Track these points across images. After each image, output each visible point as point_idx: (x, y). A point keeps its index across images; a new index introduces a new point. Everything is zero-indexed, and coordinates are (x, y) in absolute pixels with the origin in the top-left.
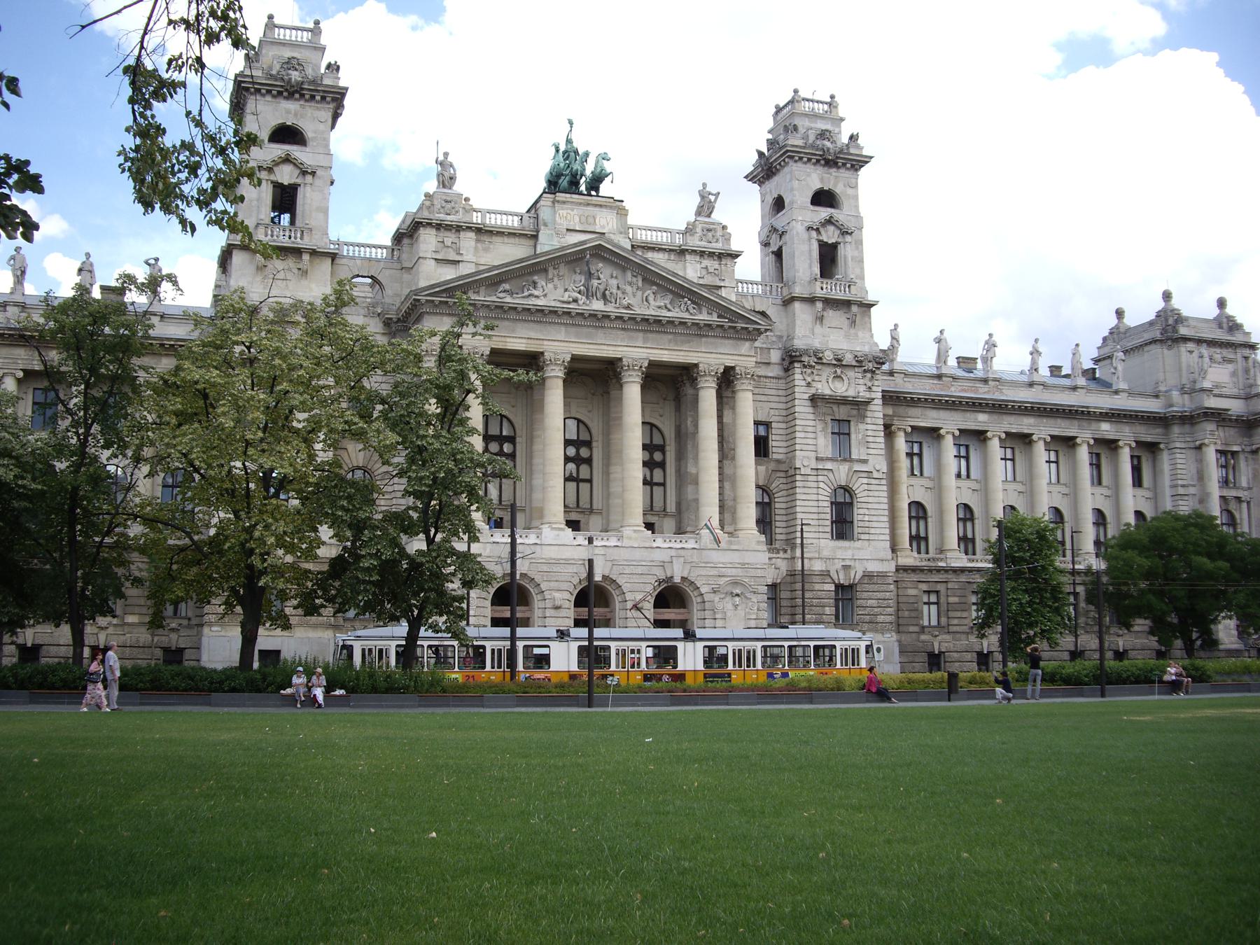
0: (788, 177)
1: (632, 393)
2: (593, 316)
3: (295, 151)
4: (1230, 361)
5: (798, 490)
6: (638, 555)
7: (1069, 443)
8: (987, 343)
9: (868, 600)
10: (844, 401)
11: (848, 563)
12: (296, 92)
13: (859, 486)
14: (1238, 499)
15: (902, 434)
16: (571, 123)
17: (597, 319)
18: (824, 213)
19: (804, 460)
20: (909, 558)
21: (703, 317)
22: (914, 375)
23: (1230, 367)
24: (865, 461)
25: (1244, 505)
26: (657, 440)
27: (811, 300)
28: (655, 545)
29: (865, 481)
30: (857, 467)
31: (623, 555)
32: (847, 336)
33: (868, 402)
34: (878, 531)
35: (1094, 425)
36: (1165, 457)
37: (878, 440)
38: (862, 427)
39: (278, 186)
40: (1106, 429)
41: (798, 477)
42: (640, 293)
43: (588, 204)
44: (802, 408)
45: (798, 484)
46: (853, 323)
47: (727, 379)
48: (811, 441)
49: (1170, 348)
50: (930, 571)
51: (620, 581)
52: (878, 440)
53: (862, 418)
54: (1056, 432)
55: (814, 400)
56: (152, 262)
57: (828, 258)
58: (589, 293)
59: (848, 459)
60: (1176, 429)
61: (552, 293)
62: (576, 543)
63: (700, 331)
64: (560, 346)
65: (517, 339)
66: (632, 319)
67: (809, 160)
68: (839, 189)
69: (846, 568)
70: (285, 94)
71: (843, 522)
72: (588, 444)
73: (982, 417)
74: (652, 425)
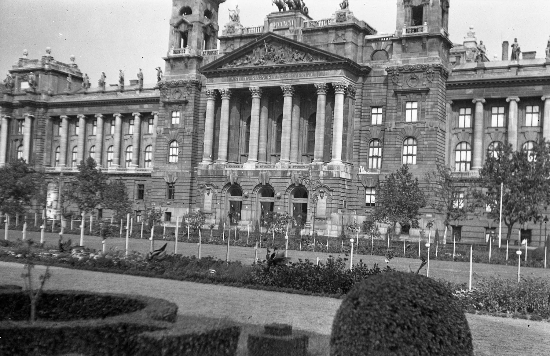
2: (266, 69)
21: (319, 61)
47: (331, 91)
50: (461, 181)
58: (268, 58)
64: (255, 84)
65: (239, 84)
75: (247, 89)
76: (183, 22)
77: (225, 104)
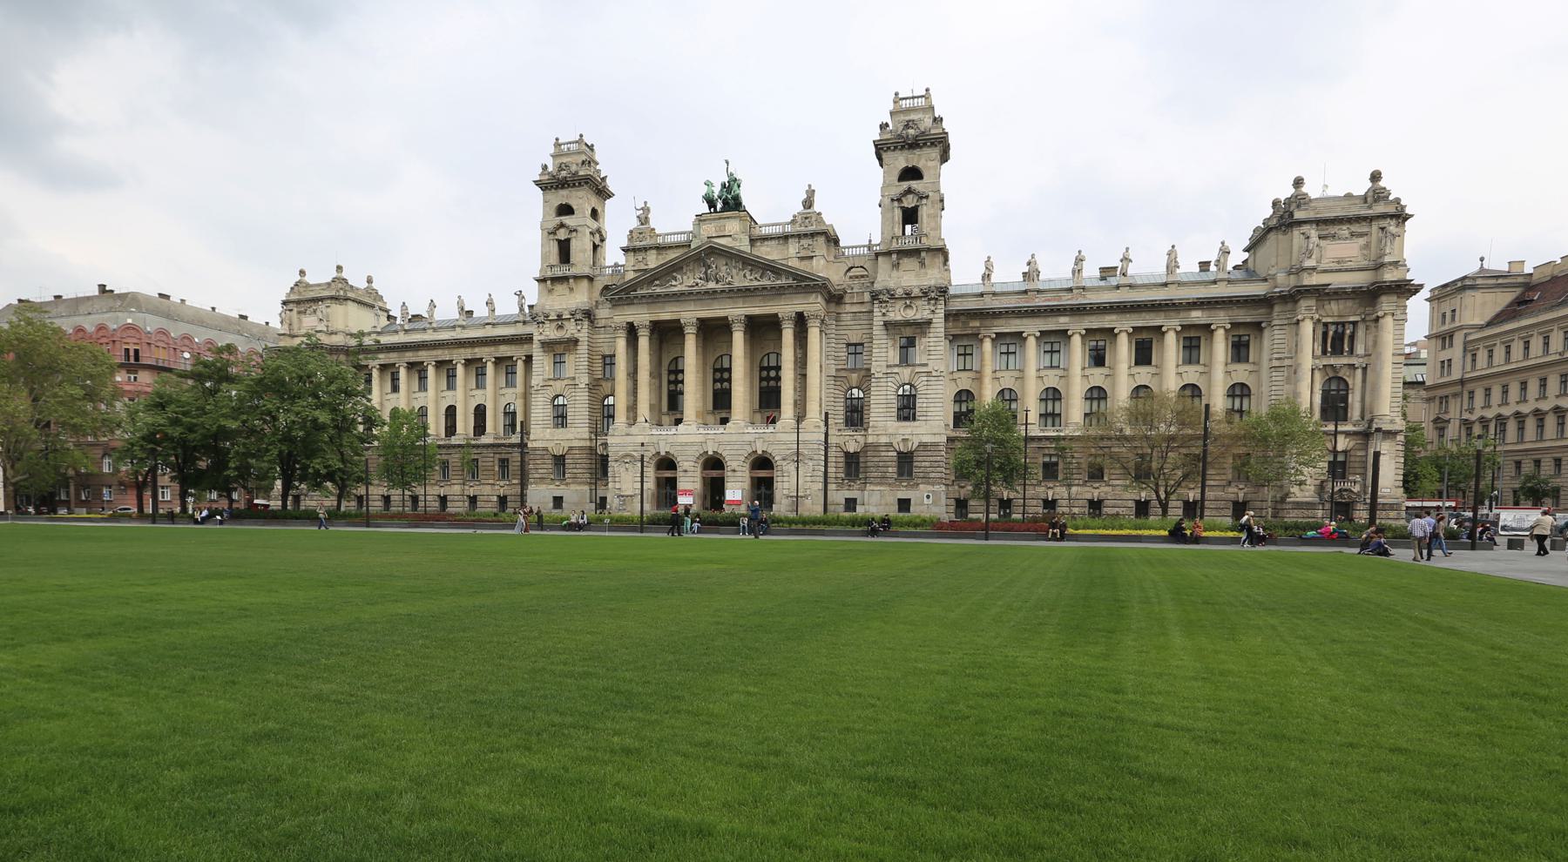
1: (738, 338)
4: (1361, 235)
6: (734, 438)
7: (1064, 334)
9: (921, 463)
10: (907, 324)
13: (921, 382)
14: (1352, 367)
17: (712, 295)
19: (877, 368)
21: (783, 281)
22: (1003, 294)
23: (1362, 241)
24: (925, 365)
25: (1359, 372)
31: (726, 438)
33: (929, 322)
35: (1182, 314)
36: (1266, 333)
39: (559, 241)
40: (1197, 316)
44: (878, 331)
46: (922, 264)
47: (801, 321)
48: (884, 353)
49: (1285, 232)
53: (924, 334)
54: (1140, 324)
55: (887, 325)
60: (1277, 308)
61: (684, 282)
63: (779, 292)
64: (689, 315)
65: (666, 314)
66: (731, 291)
71: (907, 409)
73: (1063, 320)
75: (678, 321)
76: (562, 225)
77: (644, 342)
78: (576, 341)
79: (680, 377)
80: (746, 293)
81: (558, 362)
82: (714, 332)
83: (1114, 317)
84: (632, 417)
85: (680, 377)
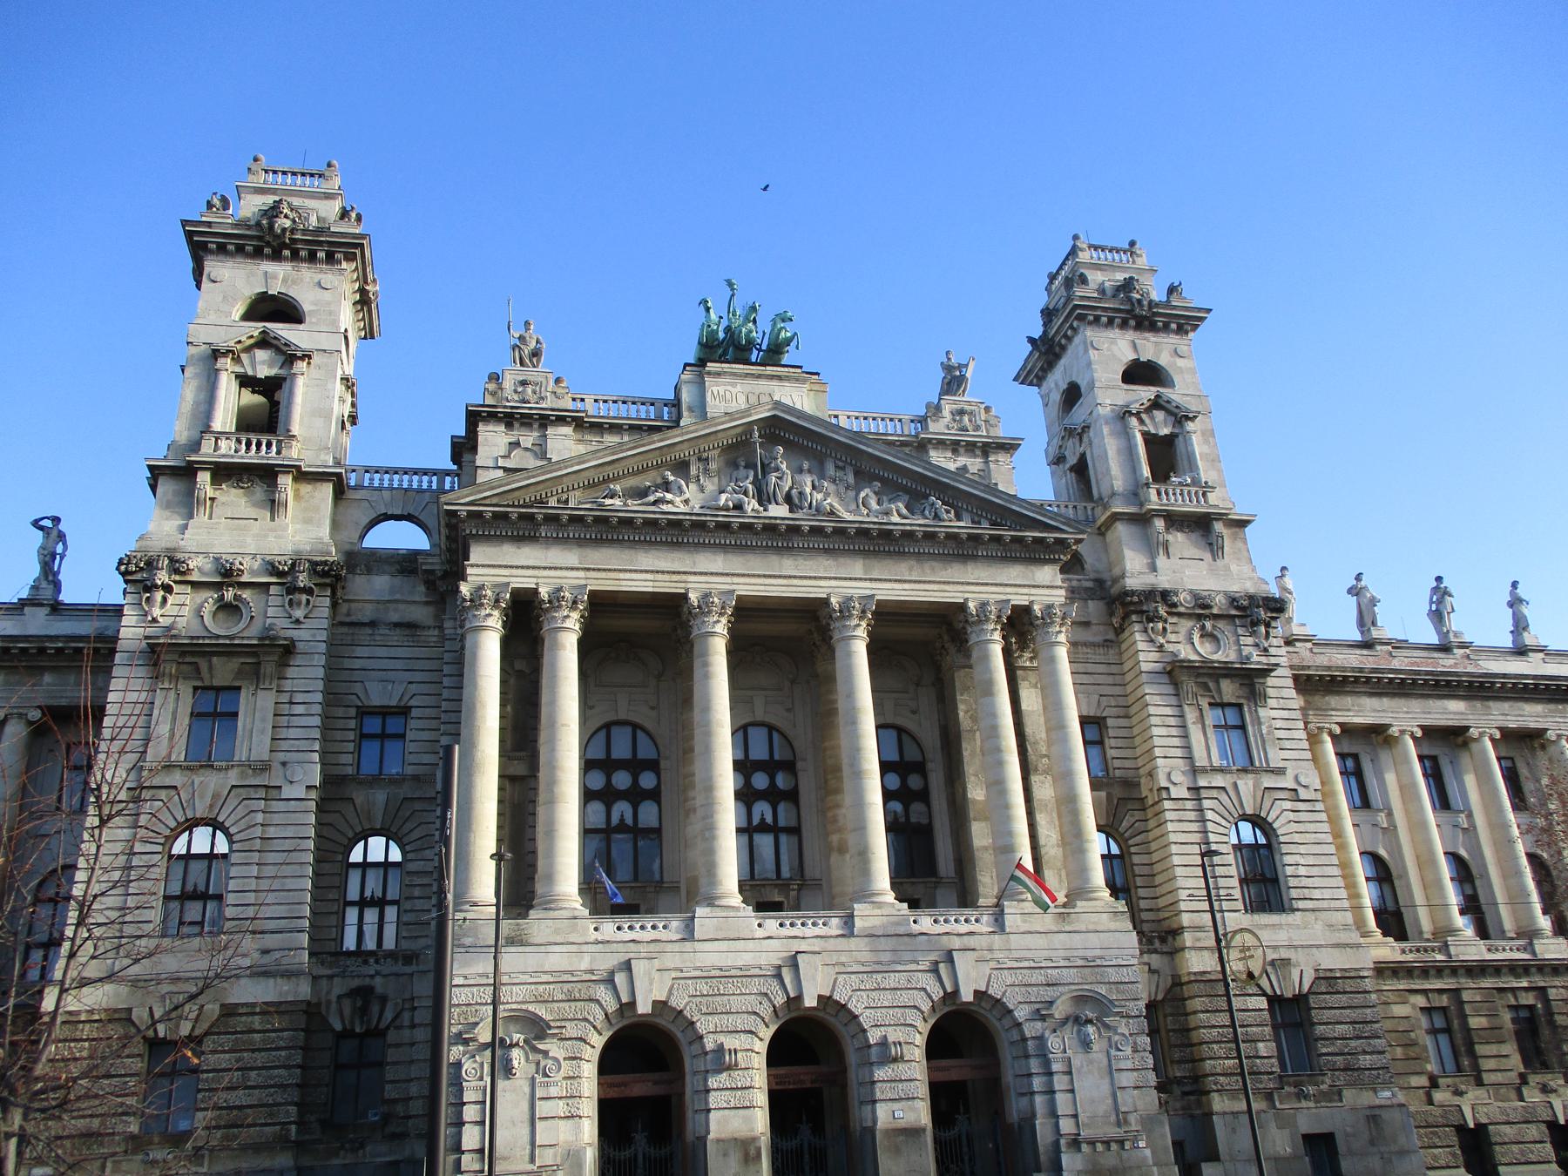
0: (1081, 348)
2: (771, 529)
3: (282, 330)
5: (1170, 827)
8: (1435, 590)
11: (1284, 954)
12: (286, 246)
15: (1328, 739)
16: (730, 284)
18: (1146, 393)
20: (1389, 950)
24: (1280, 772)
26: (912, 754)
27: (1142, 520)
28: (916, 928)
29: (1288, 805)
30: (1268, 781)
32: (1211, 570)
34: (1327, 894)
37: (1296, 734)
38: (1262, 712)
41: (1167, 804)
42: (852, 494)
43: (759, 376)
45: (1169, 815)
51: (856, 1006)
52: (1296, 734)
55: (1175, 673)
56: (48, 523)
57: (1165, 456)
59: (1249, 768)
62: (760, 933)
63: (962, 549)
65: (641, 572)
67: (1111, 322)
68: (1163, 360)
69: (1282, 964)
70: (267, 250)
71: (1265, 883)
72: (790, 766)
74: (900, 730)
78: (288, 651)
79: (597, 781)
80: (876, 543)
81: (214, 712)
82: (785, 645)
83: (1539, 708)
84: (522, 887)
85: (597, 781)
